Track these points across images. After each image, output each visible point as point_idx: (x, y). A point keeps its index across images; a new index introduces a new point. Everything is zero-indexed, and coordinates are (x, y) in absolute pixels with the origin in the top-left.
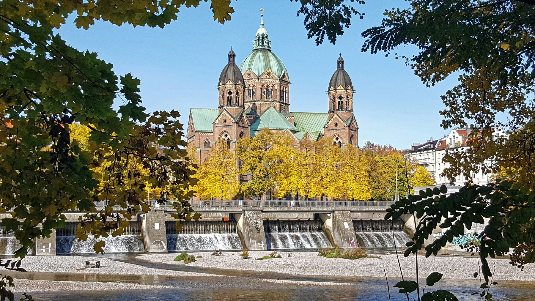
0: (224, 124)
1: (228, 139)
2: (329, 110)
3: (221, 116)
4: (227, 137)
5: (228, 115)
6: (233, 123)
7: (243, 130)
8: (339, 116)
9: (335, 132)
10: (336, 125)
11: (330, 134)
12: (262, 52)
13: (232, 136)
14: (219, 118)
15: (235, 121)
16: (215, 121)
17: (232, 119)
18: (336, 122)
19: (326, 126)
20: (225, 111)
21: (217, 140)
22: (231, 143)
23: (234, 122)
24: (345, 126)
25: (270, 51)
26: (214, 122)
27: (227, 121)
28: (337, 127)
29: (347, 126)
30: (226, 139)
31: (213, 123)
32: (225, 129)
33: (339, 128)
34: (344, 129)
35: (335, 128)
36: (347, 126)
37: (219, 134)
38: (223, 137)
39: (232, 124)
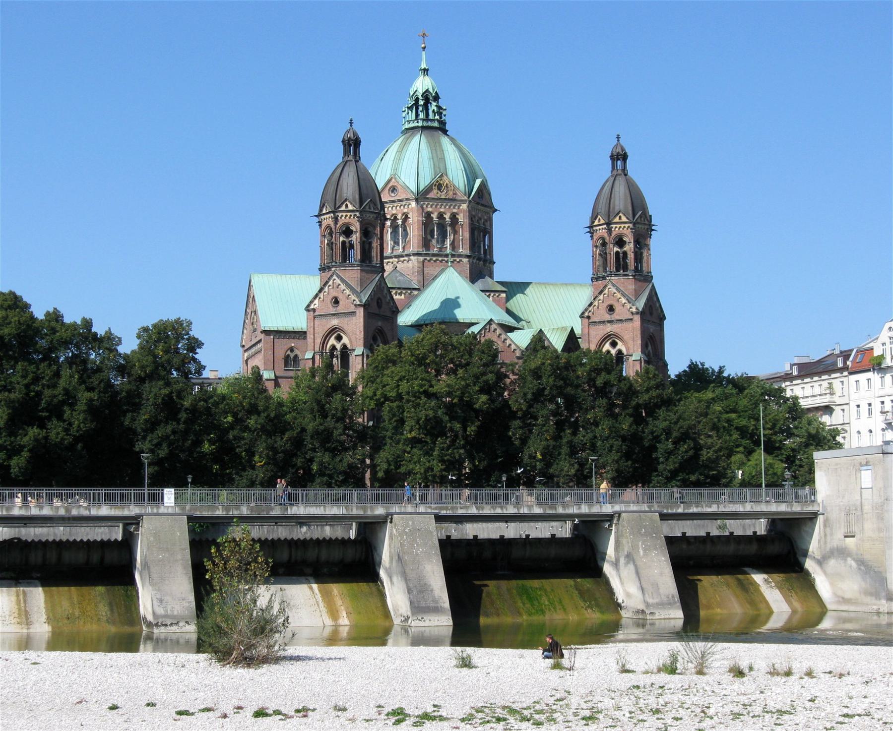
0: (332, 310)
1: (345, 347)
2: (593, 274)
3: (326, 289)
4: (342, 342)
5: (343, 287)
6: (356, 305)
7: (380, 324)
8: (618, 289)
9: (609, 328)
10: (611, 309)
11: (599, 332)
12: (426, 137)
13: (353, 339)
14: (321, 295)
15: (360, 301)
16: (311, 302)
17: (353, 297)
18: (610, 303)
19: (586, 314)
20: (335, 277)
21: (317, 349)
22: (352, 359)
23: (358, 303)
24: (632, 313)
25: (445, 132)
26: (309, 306)
27: (341, 303)
28: (612, 316)
29: (637, 313)
30: (339, 346)
31: (308, 309)
32: (335, 322)
33: (618, 318)
34: (631, 319)
35: (607, 317)
36: (637, 313)
37: (322, 335)
38: (332, 341)
39: (352, 309)
